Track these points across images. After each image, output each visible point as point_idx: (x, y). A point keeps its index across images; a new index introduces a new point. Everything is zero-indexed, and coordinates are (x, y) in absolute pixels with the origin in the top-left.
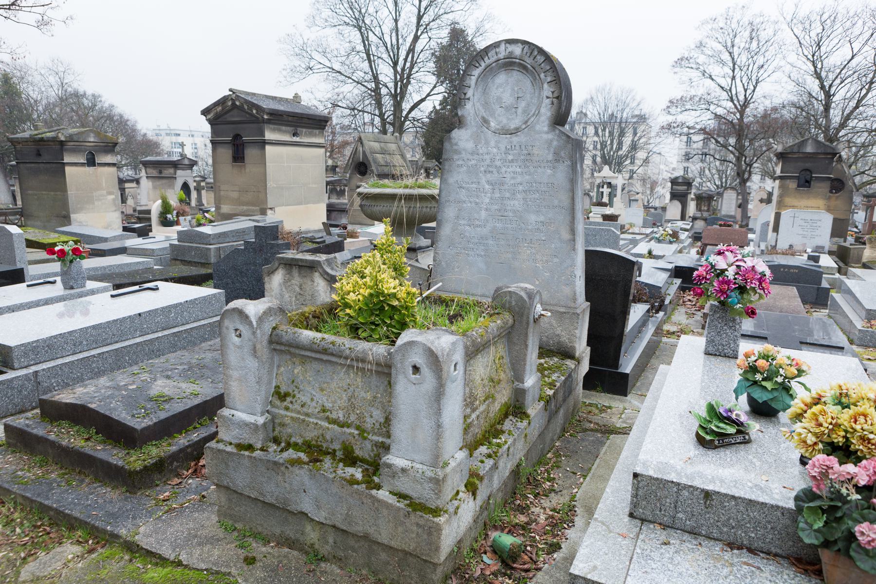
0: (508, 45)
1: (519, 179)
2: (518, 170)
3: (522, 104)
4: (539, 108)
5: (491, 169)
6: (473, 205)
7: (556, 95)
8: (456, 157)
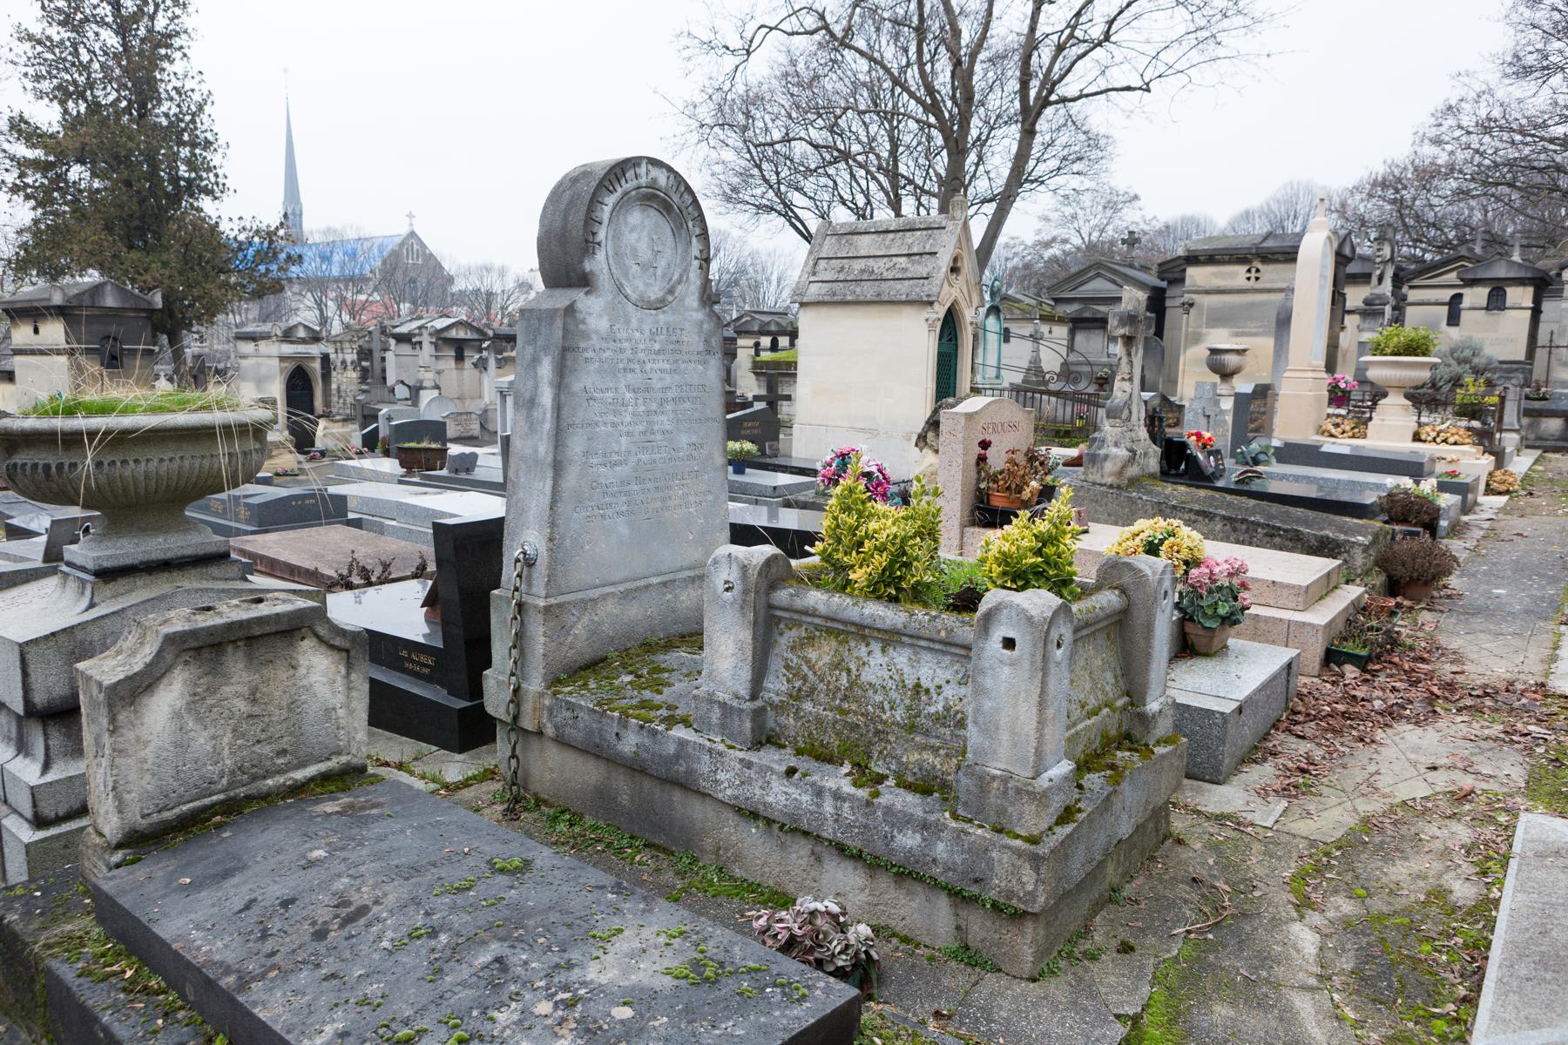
0: (650, 167)
1: (668, 380)
2: (667, 366)
3: (662, 263)
4: (686, 271)
5: (631, 366)
6: (610, 428)
7: (704, 257)
8: (582, 345)
